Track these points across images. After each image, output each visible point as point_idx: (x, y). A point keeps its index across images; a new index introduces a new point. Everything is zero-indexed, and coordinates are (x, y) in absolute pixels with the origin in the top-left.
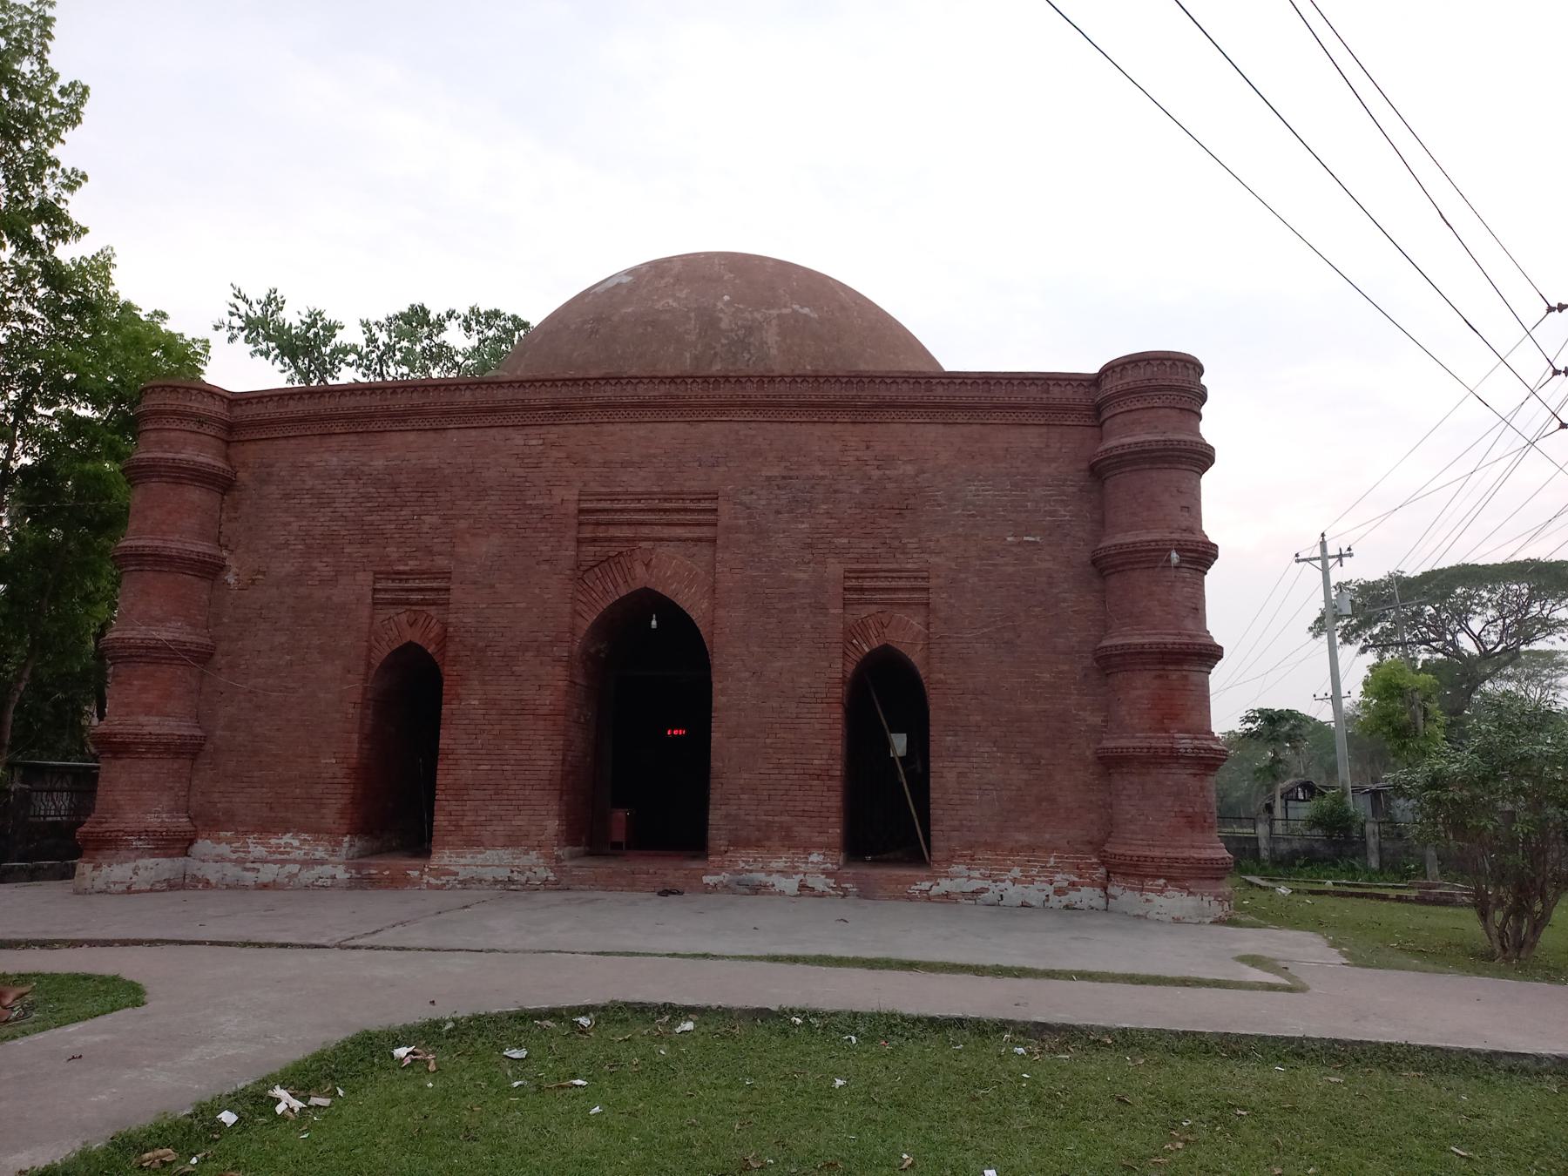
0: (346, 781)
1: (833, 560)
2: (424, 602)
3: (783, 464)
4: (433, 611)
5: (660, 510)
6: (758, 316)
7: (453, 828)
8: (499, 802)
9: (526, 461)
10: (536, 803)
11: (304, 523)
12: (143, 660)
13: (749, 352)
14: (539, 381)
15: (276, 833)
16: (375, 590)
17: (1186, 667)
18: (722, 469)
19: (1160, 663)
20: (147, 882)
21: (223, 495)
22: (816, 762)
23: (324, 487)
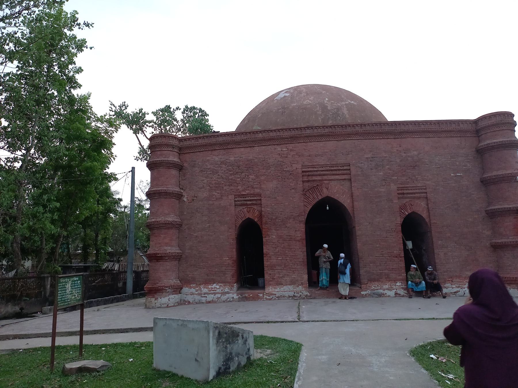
1: (393, 184)
2: (253, 204)
3: (371, 153)
4: (255, 207)
5: (330, 170)
6: (339, 105)
7: (272, 279)
8: (286, 270)
12: (164, 228)
13: (339, 117)
14: (284, 129)
18: (350, 156)
20: (173, 303)
21: (180, 171)
22: (395, 252)
23: (214, 167)
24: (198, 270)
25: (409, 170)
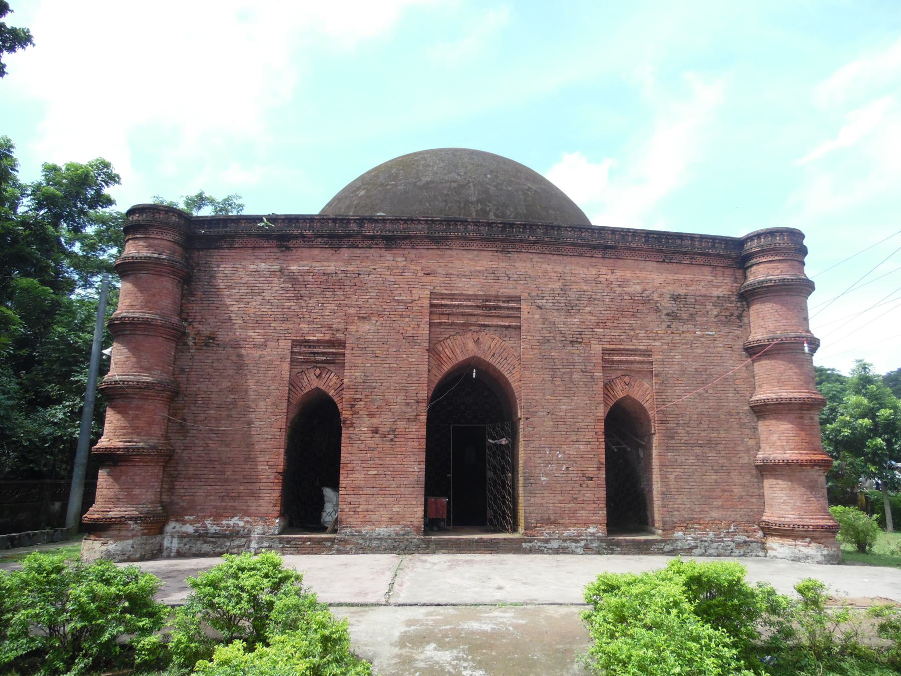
1: (595, 342)
7: (352, 513)
9: (394, 271)
10: (409, 496)
11: (243, 306)
12: (136, 397)
15: (228, 517)
16: (292, 352)
17: (813, 412)
19: (799, 409)
22: (590, 469)
24: (203, 487)
25: (625, 319)
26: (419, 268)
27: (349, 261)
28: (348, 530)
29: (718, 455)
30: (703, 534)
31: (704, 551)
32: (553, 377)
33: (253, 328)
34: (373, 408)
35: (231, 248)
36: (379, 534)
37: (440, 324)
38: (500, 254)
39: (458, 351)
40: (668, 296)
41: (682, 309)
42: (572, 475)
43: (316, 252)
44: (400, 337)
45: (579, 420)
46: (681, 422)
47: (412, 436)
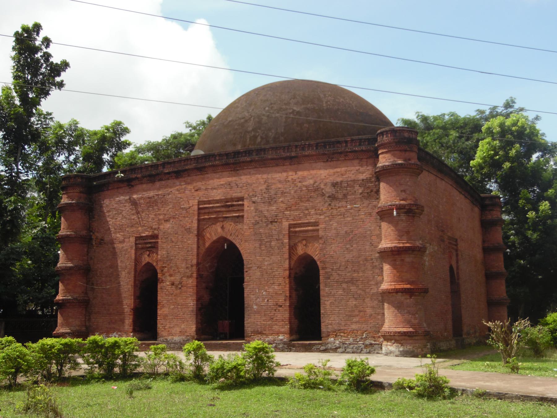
0: (131, 313)
7: (163, 329)
11: (114, 221)
16: (136, 244)
17: (403, 256)
22: (280, 300)
26: (192, 187)
27: (159, 189)
28: (161, 339)
29: (357, 288)
30: (346, 340)
31: (344, 350)
32: (260, 245)
33: (119, 232)
34: (172, 272)
35: (108, 190)
36: (175, 341)
37: (209, 218)
38: (233, 172)
39: (213, 234)
40: (331, 184)
41: (339, 192)
42: (270, 304)
43: (144, 186)
44: (183, 229)
45: (275, 271)
46: (335, 267)
47: (189, 286)
